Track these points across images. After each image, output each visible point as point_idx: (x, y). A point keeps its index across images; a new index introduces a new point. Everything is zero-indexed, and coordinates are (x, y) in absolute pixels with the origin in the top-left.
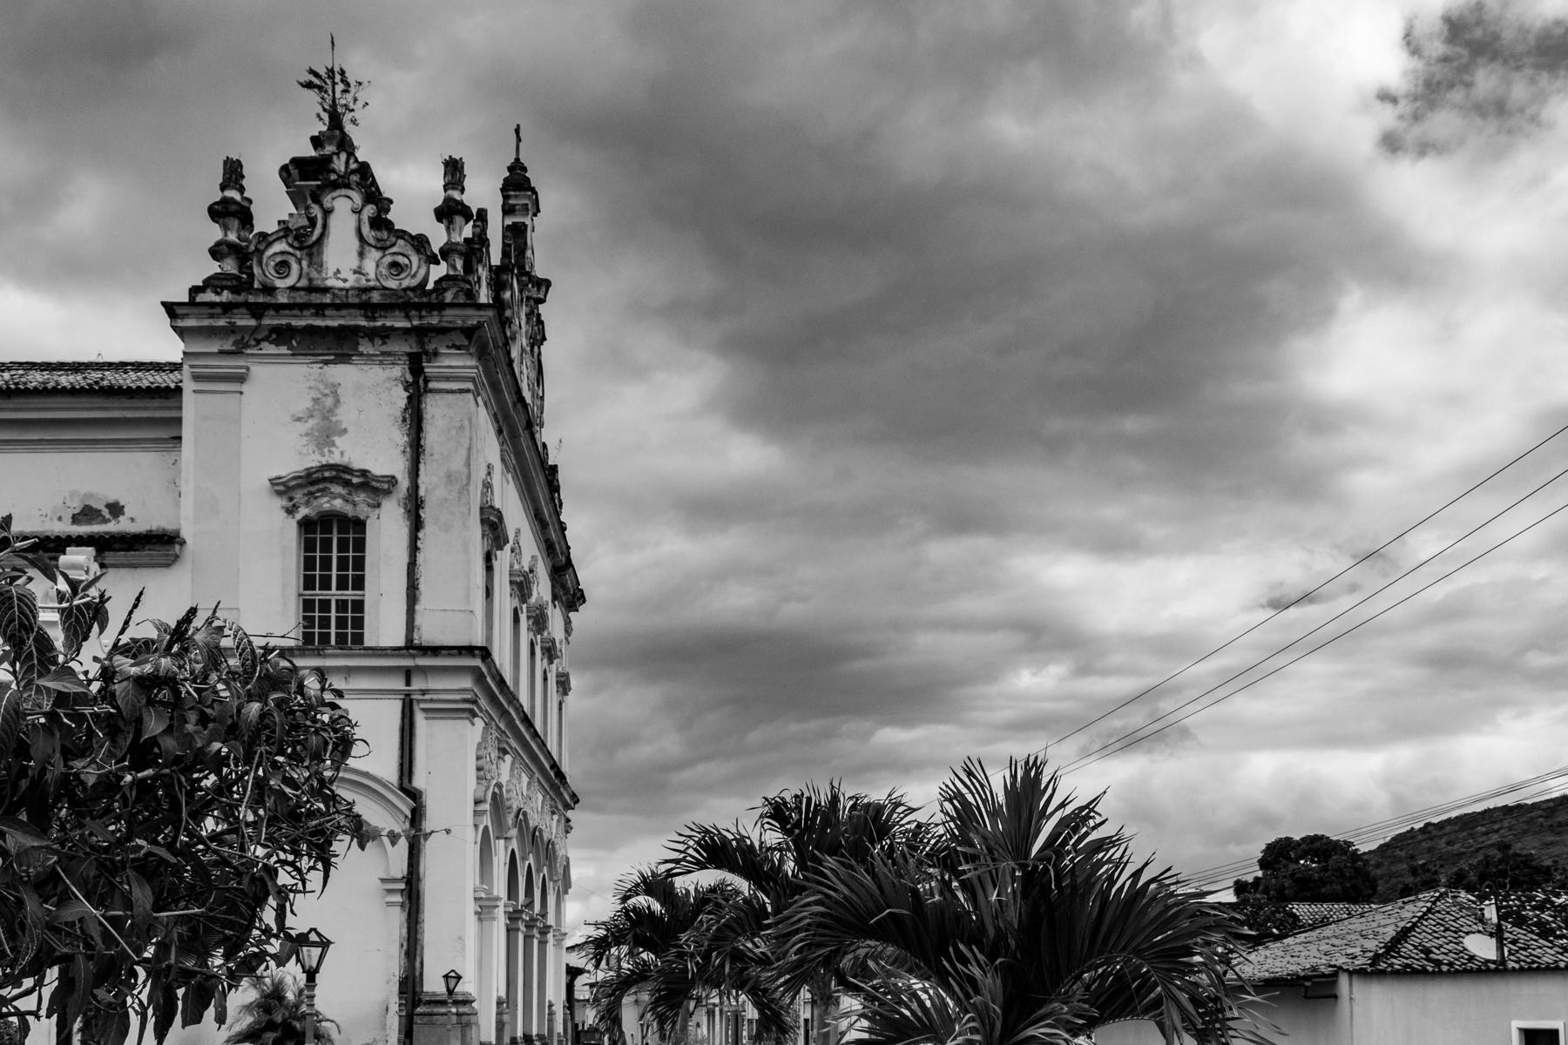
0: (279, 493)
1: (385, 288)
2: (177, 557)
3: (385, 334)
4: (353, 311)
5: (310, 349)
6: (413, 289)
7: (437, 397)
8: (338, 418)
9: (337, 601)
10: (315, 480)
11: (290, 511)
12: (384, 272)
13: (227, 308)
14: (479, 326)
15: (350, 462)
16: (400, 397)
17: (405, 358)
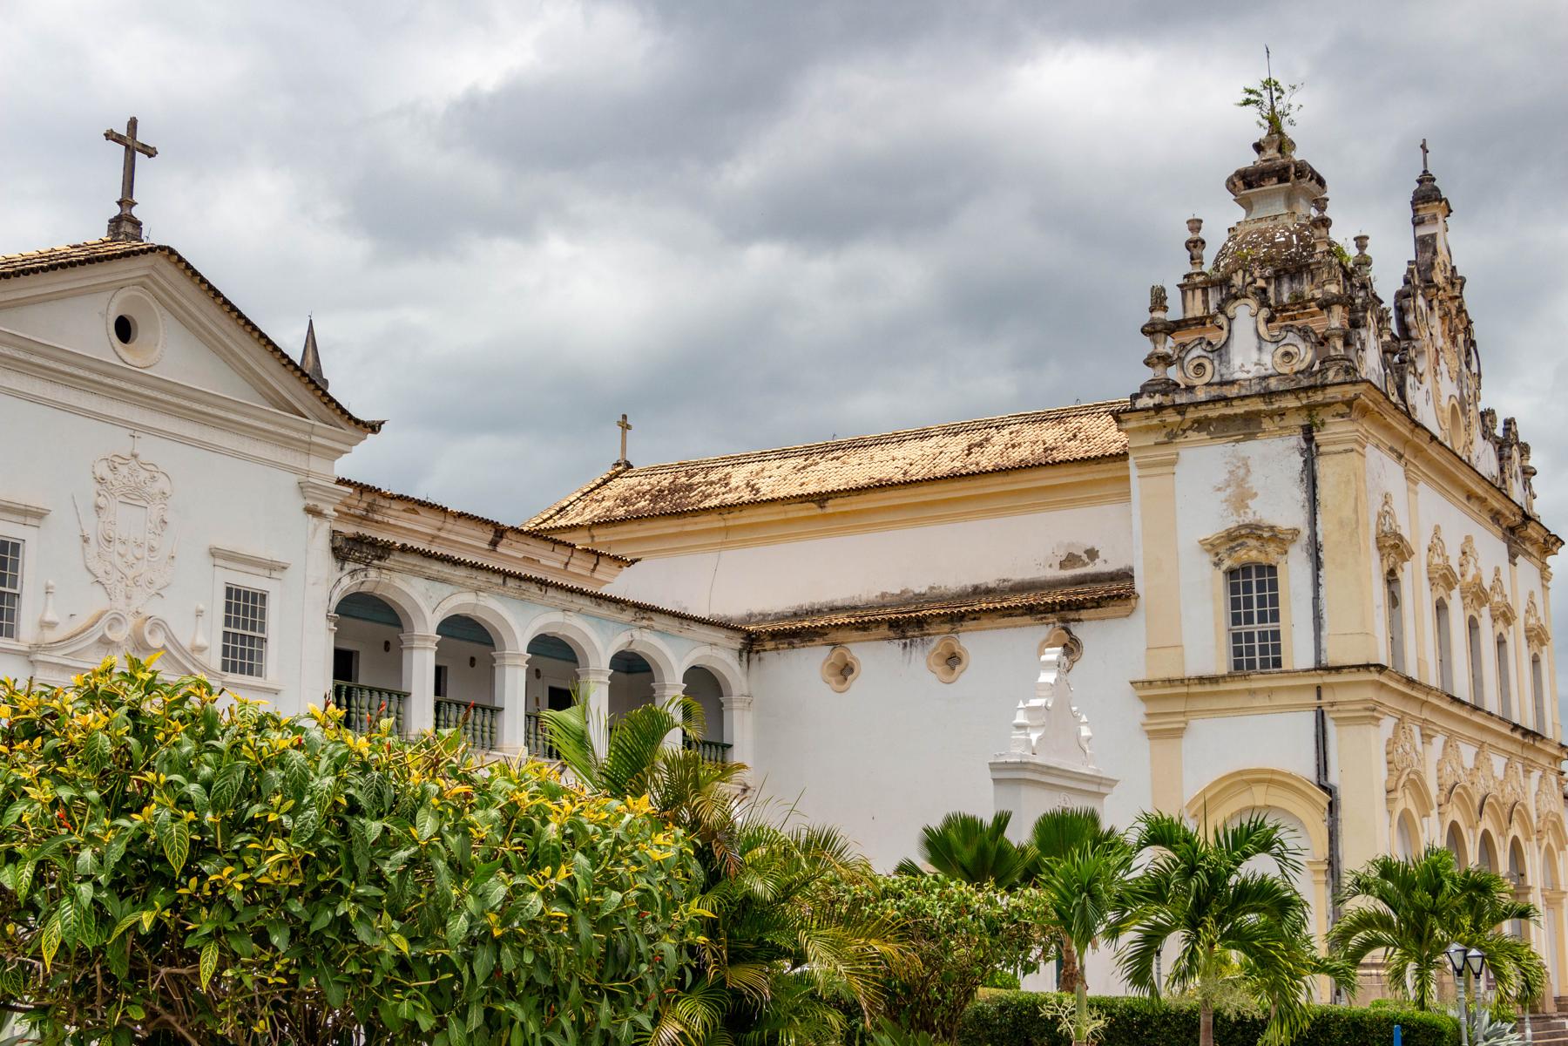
0: (1208, 551)
1: (1280, 374)
3: (1282, 413)
4: (1254, 399)
5: (1224, 432)
6: (1301, 372)
7: (1327, 458)
8: (1250, 485)
9: (1259, 632)
10: (1234, 538)
11: (1216, 565)
12: (1279, 361)
13: (1159, 408)
14: (1357, 397)
16: (1298, 462)
17: (1300, 430)
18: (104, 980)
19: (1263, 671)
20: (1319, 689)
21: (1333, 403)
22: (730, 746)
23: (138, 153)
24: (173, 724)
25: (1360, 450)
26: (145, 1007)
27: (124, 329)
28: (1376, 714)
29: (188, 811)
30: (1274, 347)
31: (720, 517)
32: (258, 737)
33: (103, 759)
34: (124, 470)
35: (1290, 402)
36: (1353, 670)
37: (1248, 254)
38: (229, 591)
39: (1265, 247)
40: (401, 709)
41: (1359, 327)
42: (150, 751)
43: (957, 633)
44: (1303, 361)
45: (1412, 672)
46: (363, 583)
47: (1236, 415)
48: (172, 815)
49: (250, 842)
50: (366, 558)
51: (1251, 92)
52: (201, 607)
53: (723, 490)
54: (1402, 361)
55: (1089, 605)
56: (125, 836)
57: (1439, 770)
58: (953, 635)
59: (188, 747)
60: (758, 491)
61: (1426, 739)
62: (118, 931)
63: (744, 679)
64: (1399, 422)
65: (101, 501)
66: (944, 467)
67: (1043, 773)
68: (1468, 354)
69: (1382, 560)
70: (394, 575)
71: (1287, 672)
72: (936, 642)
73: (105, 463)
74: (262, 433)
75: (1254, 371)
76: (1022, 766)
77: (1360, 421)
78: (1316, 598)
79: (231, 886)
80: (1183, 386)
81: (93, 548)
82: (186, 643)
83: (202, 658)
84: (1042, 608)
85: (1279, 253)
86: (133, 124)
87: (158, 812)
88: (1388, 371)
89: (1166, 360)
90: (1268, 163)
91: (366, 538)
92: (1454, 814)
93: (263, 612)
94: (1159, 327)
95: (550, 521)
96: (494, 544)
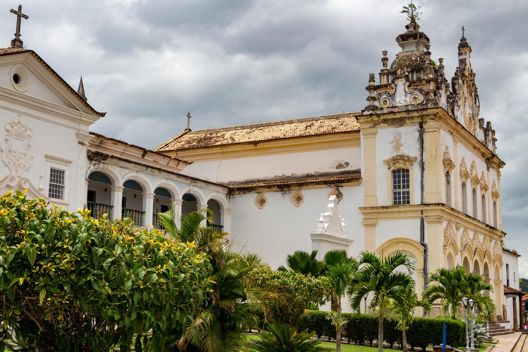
0: (386, 164)
1: (412, 105)
3: (412, 118)
4: (403, 113)
5: (393, 124)
7: (427, 133)
8: (400, 142)
9: (403, 192)
10: (395, 160)
11: (389, 169)
13: (371, 115)
14: (438, 113)
15: (404, 154)
16: (417, 134)
17: (418, 124)
18: (6, 301)
19: (403, 205)
20: (422, 211)
21: (430, 115)
22: (223, 226)
23: (22, 17)
24: (31, 214)
25: (438, 131)
26: (20, 311)
27: (16, 79)
28: (441, 220)
29: (36, 244)
30: (410, 95)
31: (221, 149)
32: (61, 219)
33: (7, 225)
34: (16, 127)
35: (415, 114)
36: (434, 205)
37: (402, 63)
38: (52, 170)
39: (408, 61)
40: (110, 212)
41: (439, 89)
42: (23, 223)
43: (301, 190)
44: (420, 100)
45: (453, 206)
46: (98, 168)
47: (397, 118)
48: (31, 245)
49: (57, 255)
50: (99, 160)
51: (405, 8)
52: (42, 175)
54: (453, 101)
55: (346, 181)
56: (14, 252)
57: (461, 240)
58: (299, 190)
59: (36, 222)
60: (234, 140)
61: (457, 229)
62: (12, 284)
63: (228, 204)
64: (452, 122)
65: (8, 138)
66: (298, 133)
67: (328, 238)
68: (476, 99)
69: (444, 168)
70: (108, 165)
71: (412, 205)
72: (294, 192)
73: (9, 125)
74: (64, 116)
75: (403, 103)
76: (321, 235)
77: (439, 121)
78: (422, 181)
79: (51, 270)
80: (379, 108)
81: (4, 154)
82: (36, 187)
83: (42, 193)
84: (330, 182)
85: (413, 63)
86: (20, 7)
87: (25, 244)
88: (449, 104)
89: (374, 99)
90: (410, 33)
91: (99, 153)
92: (466, 254)
93: (63, 177)
94: (372, 88)
95: (163, 149)
96: (143, 156)
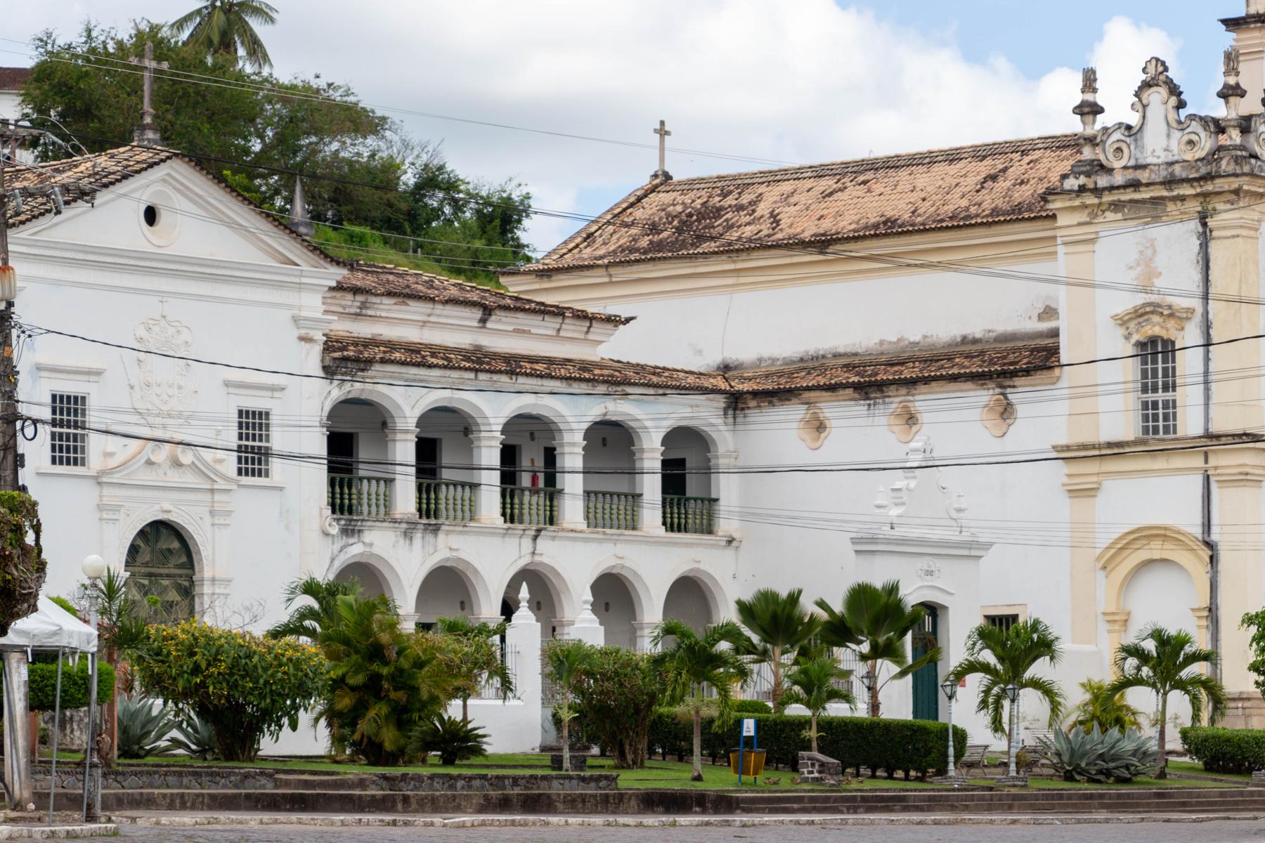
0: (1121, 325)
1: (1185, 161)
2: (1059, 378)
3: (1182, 199)
6: (1201, 160)
7: (1219, 242)
10: (1140, 314)
11: (1127, 337)
13: (1082, 189)
16: (1195, 243)
20: (1206, 454)
22: (717, 500)
35: (1186, 190)
38: (240, 412)
46: (349, 392)
53: (748, 219)
63: (729, 436)
66: (957, 202)
72: (896, 401)
75: (1164, 157)
95: (576, 251)
96: (483, 321)
